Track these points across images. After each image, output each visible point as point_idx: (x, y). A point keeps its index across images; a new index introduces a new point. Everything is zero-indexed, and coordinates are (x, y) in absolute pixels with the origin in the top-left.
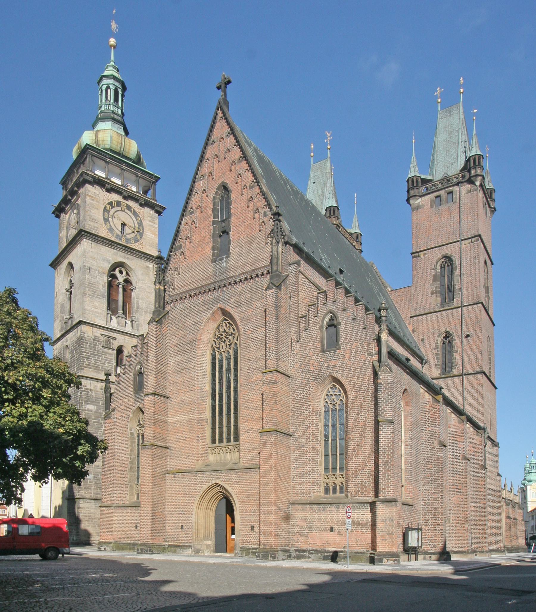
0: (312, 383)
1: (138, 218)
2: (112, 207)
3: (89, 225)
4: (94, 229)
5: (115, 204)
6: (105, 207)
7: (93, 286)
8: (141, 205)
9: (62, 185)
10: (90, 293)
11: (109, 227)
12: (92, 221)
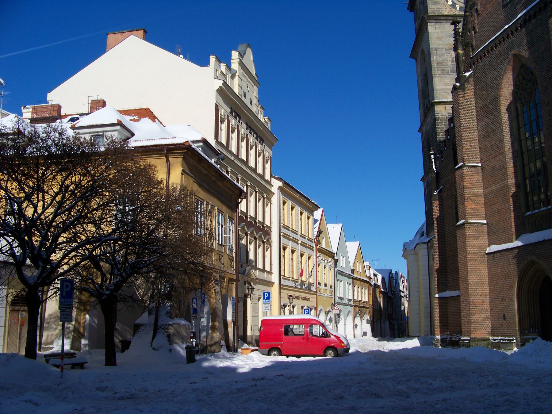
3: (431, 9)
4: (437, 11)
7: (441, 65)
10: (439, 72)
12: (434, 5)
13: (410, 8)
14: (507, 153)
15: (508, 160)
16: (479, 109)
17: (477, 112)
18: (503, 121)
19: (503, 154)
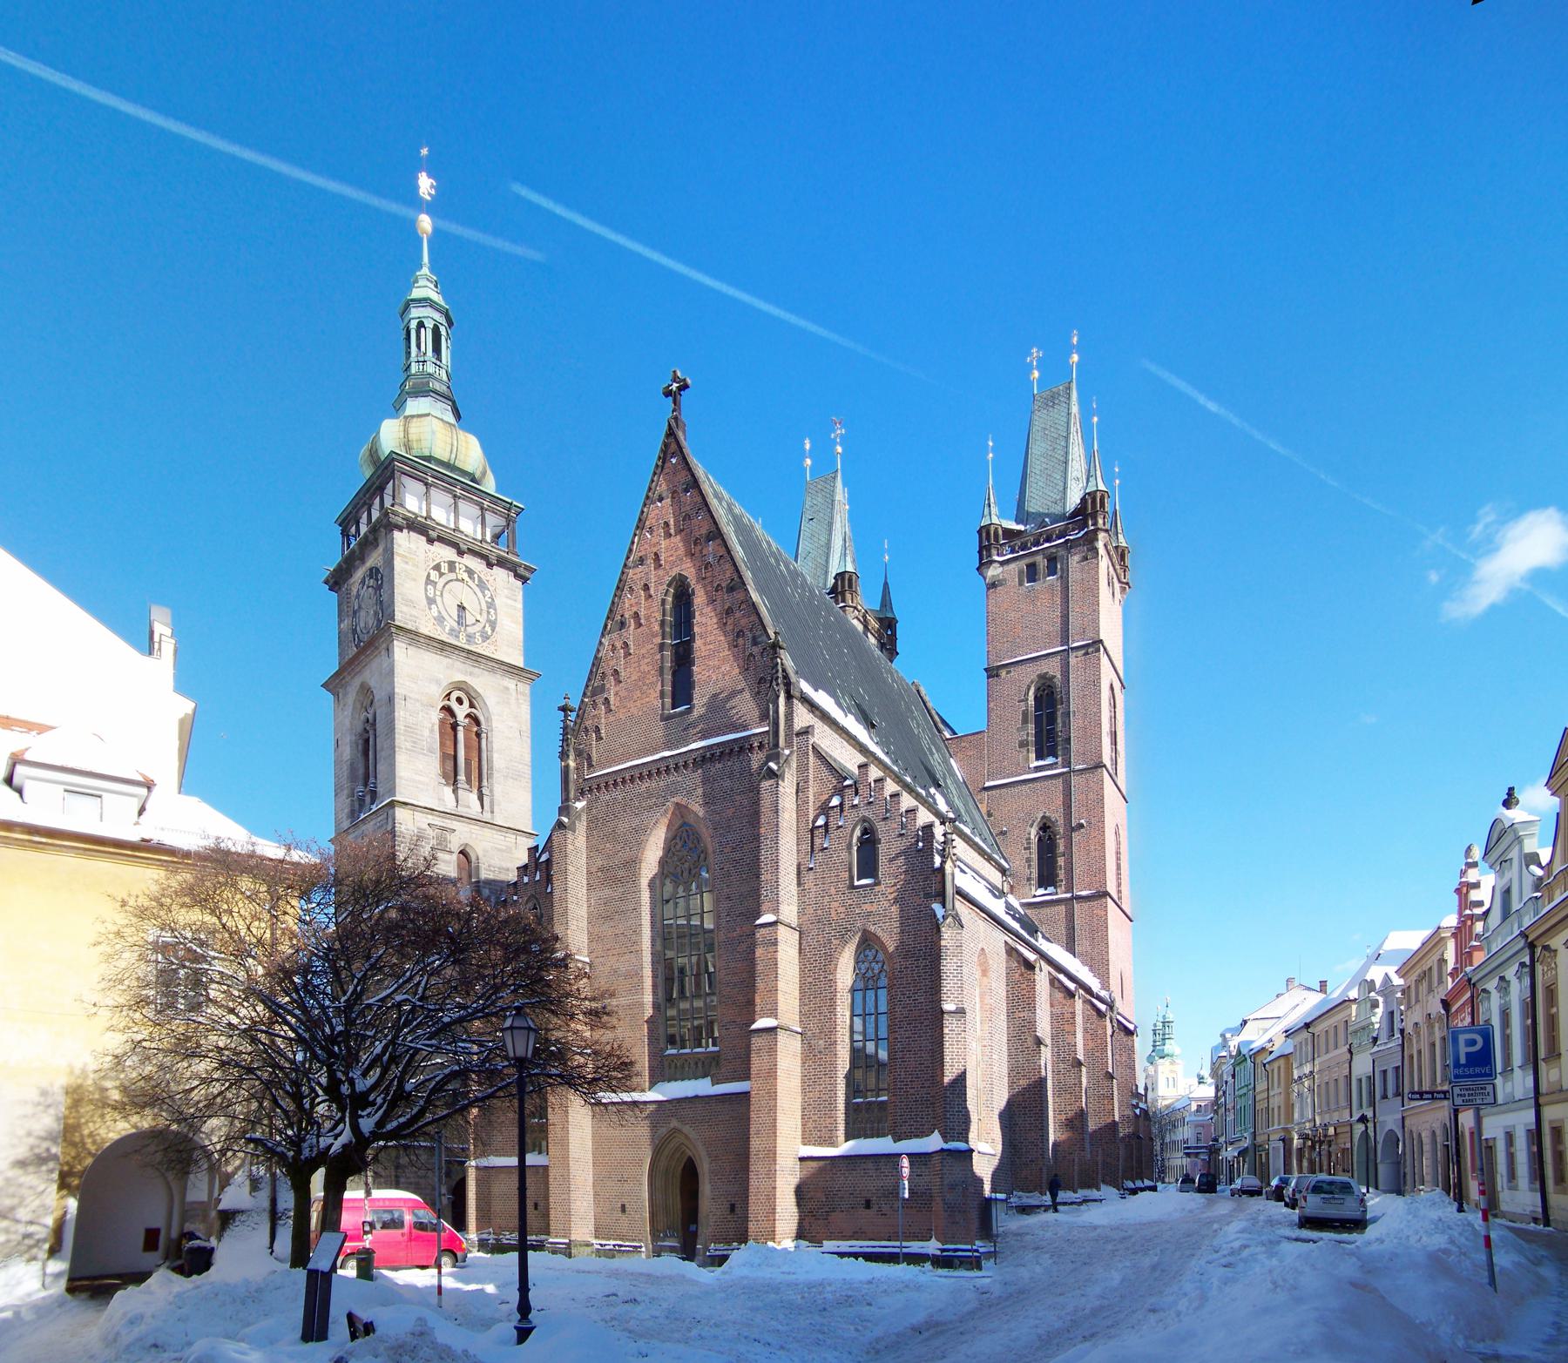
0: (835, 942)
1: (486, 592)
2: (441, 575)
5: (444, 567)
6: (429, 575)
8: (490, 565)
9: (340, 525)
11: (436, 614)
13: (332, 581)
14: (644, 953)
15: (645, 965)
16: (594, 870)
17: (589, 873)
18: (643, 902)
19: (639, 952)
